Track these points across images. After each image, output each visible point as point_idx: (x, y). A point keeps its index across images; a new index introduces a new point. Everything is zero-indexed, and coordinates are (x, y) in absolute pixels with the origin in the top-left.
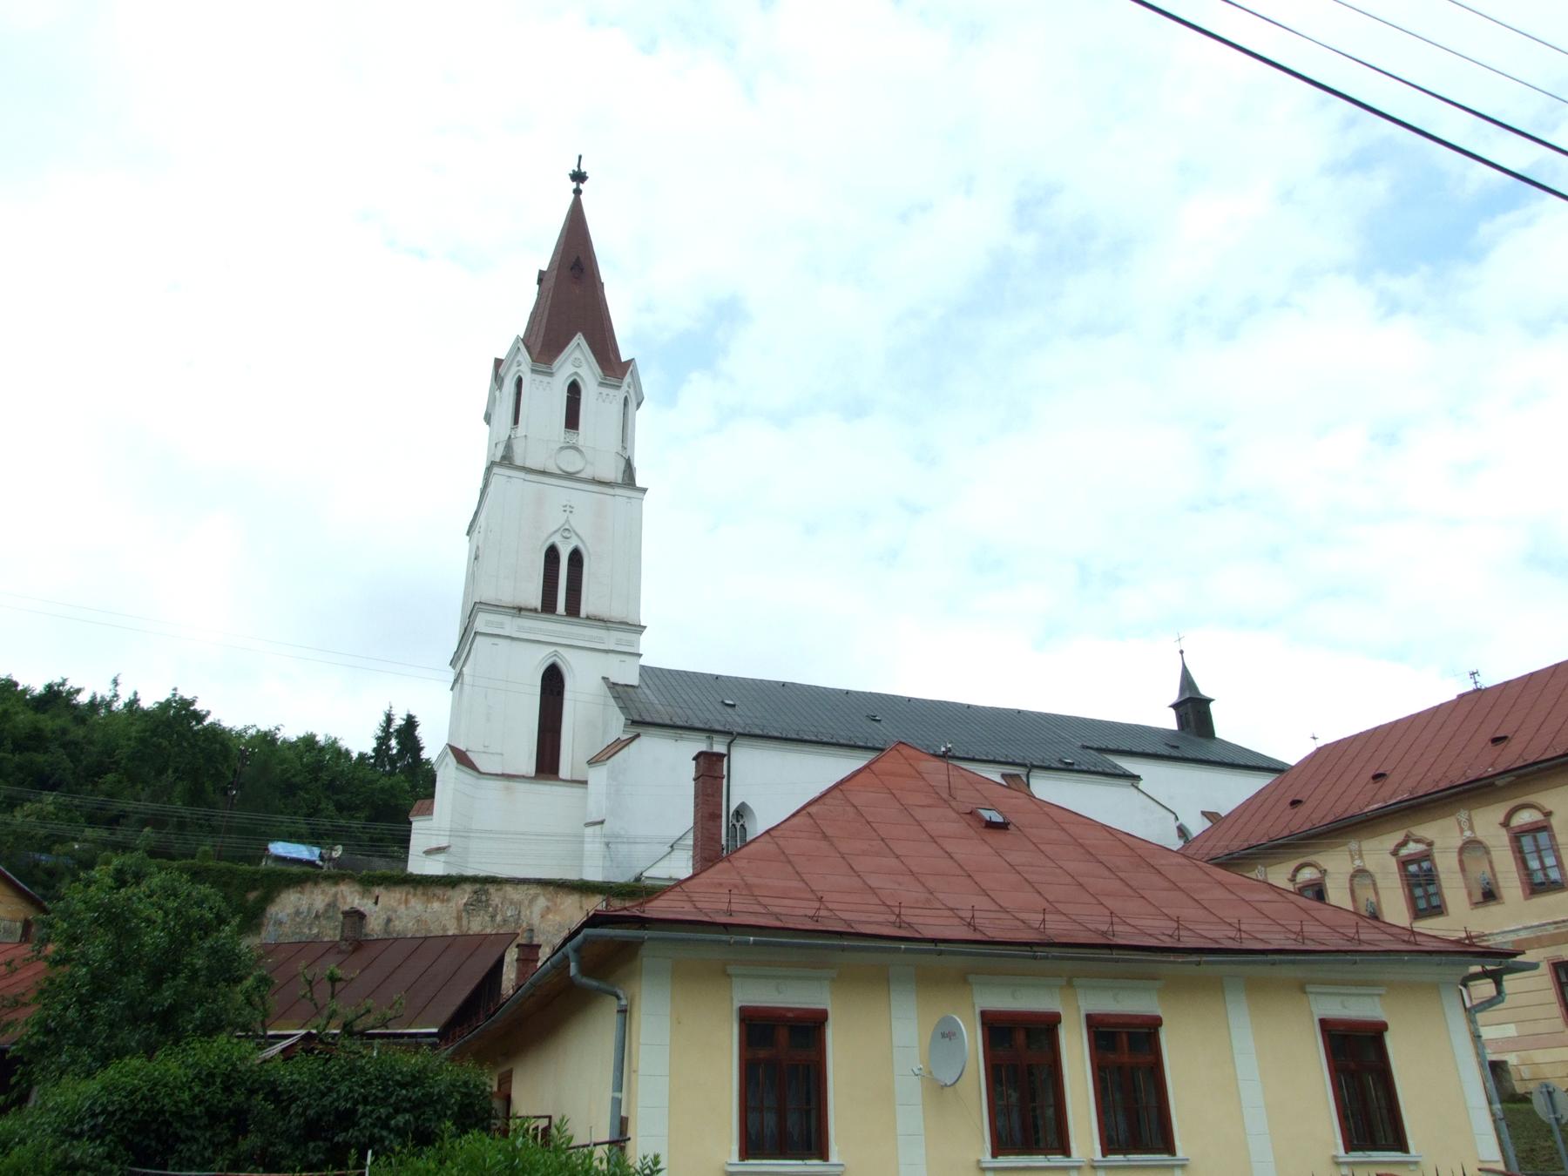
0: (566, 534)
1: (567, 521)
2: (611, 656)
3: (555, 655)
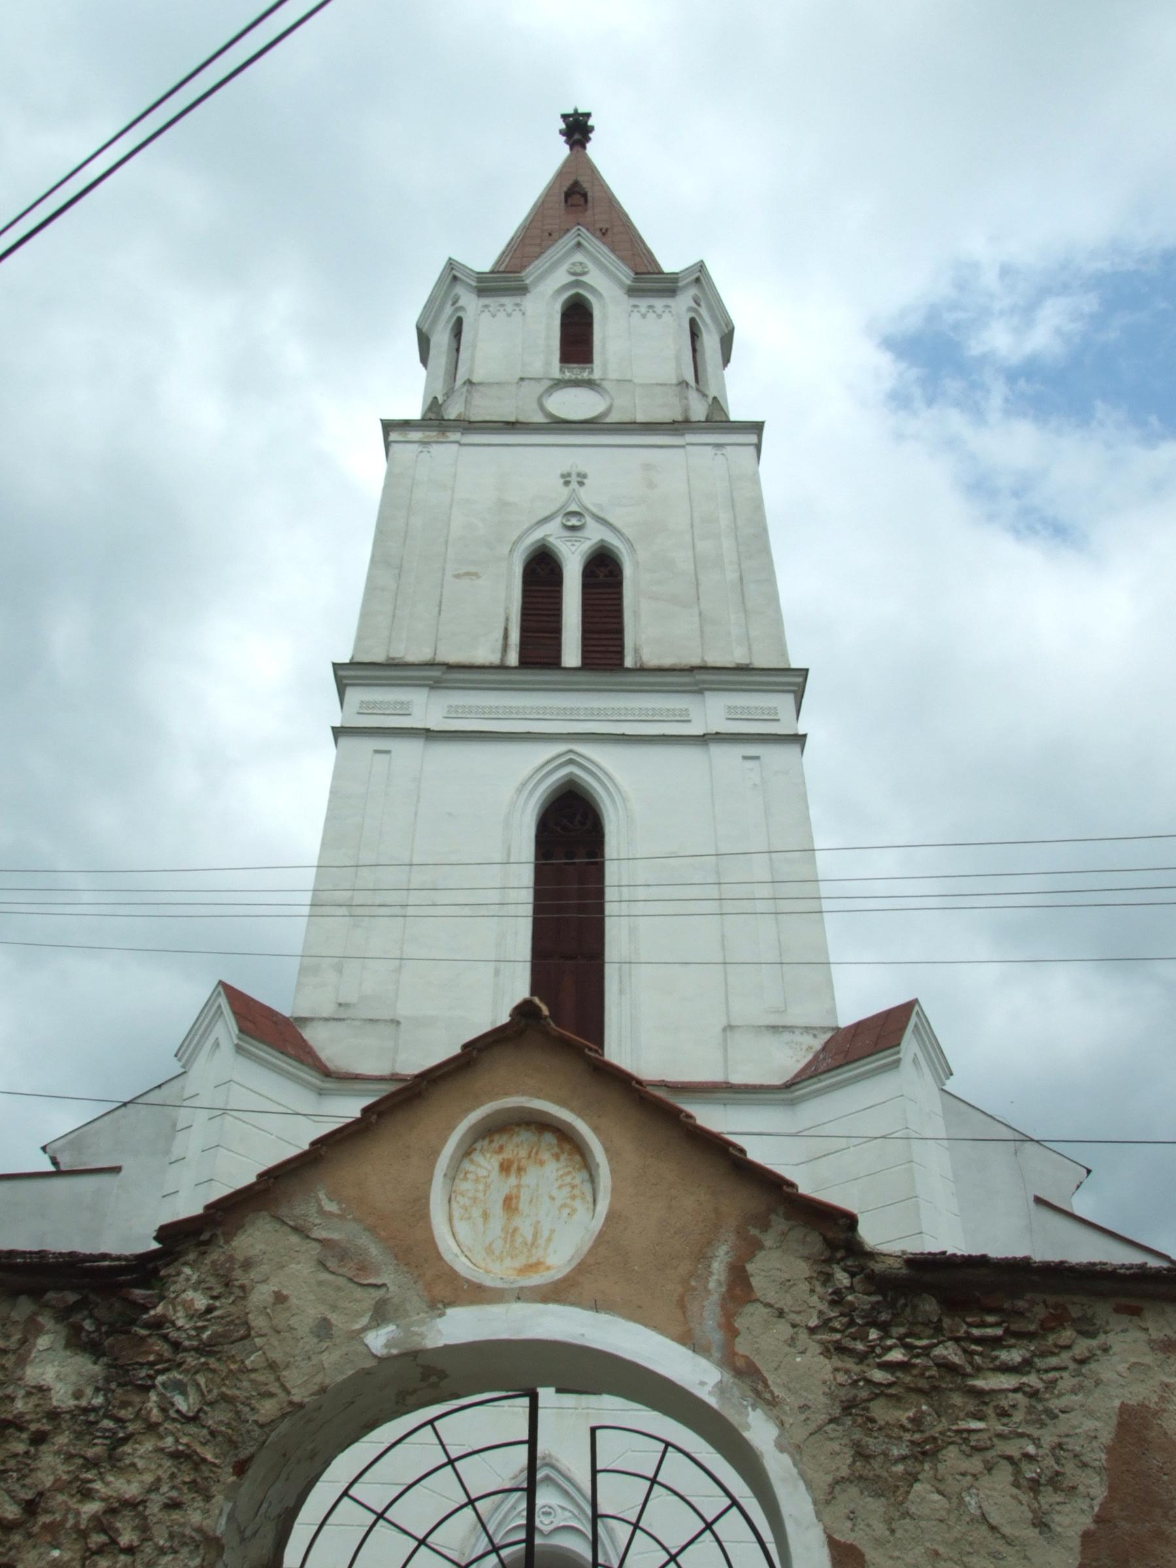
0: (574, 521)
1: (573, 497)
2: (716, 750)
3: (571, 762)
